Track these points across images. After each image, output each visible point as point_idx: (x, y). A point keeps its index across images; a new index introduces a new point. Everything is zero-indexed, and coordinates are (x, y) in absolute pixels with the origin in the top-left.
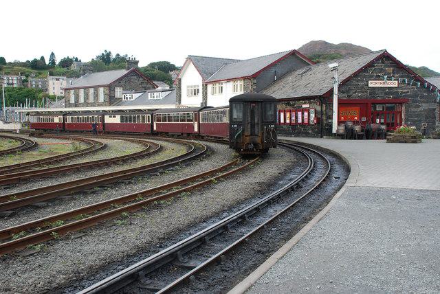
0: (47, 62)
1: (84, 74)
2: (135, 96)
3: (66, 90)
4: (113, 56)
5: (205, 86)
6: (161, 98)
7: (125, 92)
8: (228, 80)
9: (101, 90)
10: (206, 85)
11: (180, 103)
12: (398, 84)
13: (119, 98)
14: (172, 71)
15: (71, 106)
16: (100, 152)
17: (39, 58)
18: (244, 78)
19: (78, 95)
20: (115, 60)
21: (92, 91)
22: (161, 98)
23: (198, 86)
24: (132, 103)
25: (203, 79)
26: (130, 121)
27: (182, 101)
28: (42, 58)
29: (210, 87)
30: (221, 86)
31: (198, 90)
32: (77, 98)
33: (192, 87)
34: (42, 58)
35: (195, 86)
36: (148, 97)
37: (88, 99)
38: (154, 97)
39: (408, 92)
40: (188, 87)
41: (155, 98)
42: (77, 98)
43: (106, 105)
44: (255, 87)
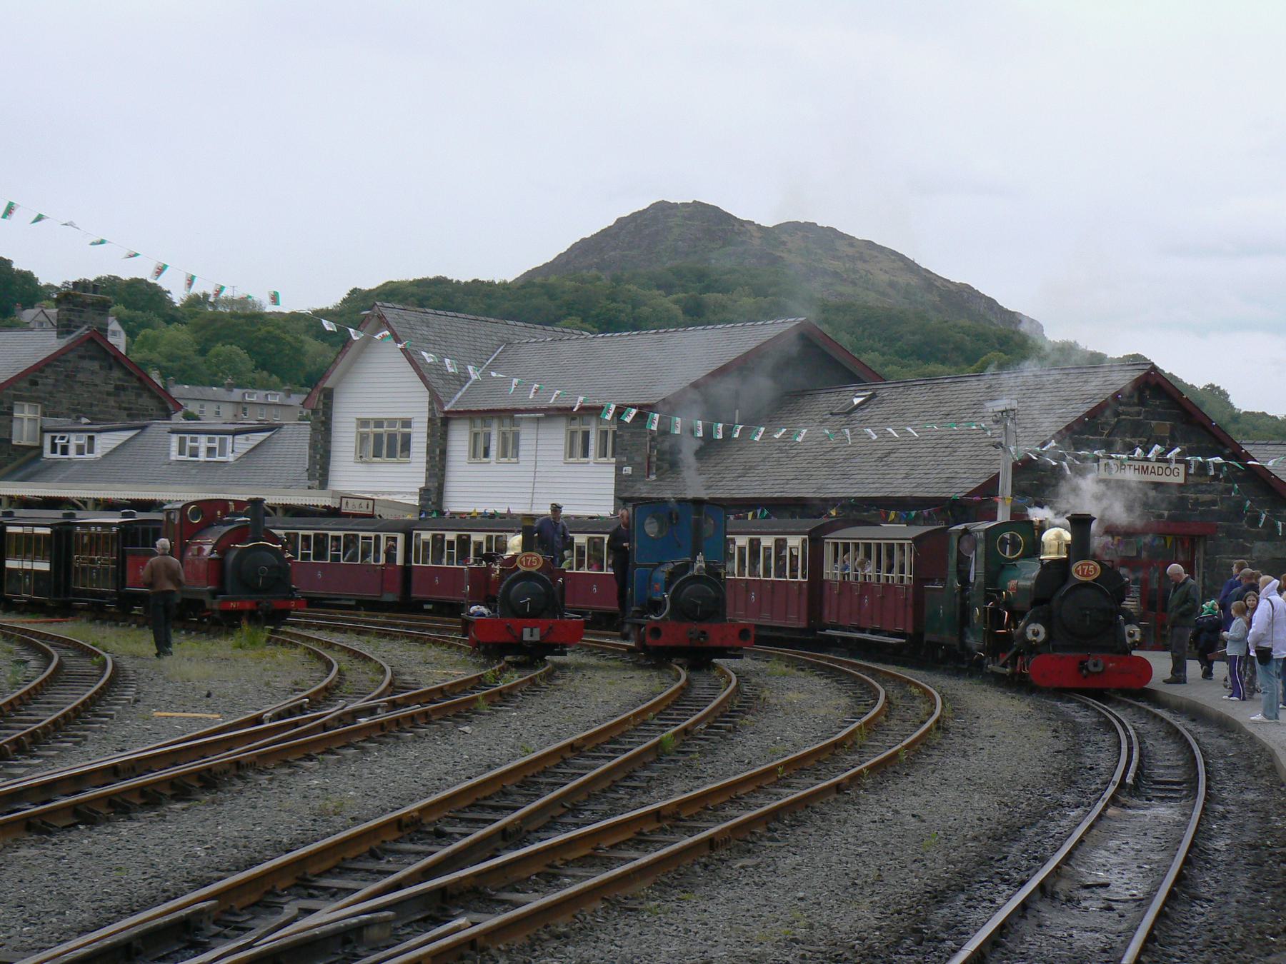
2: (106, 442)
5: (440, 425)
7: (50, 422)
11: (323, 484)
12: (1187, 474)
13: (28, 448)
14: (30, 304)
22: (230, 458)
23: (407, 423)
24: (90, 472)
25: (435, 399)
29: (460, 439)
33: (379, 423)
35: (392, 422)
38: (194, 453)
39: (1214, 503)
40: (364, 423)
41: (202, 457)
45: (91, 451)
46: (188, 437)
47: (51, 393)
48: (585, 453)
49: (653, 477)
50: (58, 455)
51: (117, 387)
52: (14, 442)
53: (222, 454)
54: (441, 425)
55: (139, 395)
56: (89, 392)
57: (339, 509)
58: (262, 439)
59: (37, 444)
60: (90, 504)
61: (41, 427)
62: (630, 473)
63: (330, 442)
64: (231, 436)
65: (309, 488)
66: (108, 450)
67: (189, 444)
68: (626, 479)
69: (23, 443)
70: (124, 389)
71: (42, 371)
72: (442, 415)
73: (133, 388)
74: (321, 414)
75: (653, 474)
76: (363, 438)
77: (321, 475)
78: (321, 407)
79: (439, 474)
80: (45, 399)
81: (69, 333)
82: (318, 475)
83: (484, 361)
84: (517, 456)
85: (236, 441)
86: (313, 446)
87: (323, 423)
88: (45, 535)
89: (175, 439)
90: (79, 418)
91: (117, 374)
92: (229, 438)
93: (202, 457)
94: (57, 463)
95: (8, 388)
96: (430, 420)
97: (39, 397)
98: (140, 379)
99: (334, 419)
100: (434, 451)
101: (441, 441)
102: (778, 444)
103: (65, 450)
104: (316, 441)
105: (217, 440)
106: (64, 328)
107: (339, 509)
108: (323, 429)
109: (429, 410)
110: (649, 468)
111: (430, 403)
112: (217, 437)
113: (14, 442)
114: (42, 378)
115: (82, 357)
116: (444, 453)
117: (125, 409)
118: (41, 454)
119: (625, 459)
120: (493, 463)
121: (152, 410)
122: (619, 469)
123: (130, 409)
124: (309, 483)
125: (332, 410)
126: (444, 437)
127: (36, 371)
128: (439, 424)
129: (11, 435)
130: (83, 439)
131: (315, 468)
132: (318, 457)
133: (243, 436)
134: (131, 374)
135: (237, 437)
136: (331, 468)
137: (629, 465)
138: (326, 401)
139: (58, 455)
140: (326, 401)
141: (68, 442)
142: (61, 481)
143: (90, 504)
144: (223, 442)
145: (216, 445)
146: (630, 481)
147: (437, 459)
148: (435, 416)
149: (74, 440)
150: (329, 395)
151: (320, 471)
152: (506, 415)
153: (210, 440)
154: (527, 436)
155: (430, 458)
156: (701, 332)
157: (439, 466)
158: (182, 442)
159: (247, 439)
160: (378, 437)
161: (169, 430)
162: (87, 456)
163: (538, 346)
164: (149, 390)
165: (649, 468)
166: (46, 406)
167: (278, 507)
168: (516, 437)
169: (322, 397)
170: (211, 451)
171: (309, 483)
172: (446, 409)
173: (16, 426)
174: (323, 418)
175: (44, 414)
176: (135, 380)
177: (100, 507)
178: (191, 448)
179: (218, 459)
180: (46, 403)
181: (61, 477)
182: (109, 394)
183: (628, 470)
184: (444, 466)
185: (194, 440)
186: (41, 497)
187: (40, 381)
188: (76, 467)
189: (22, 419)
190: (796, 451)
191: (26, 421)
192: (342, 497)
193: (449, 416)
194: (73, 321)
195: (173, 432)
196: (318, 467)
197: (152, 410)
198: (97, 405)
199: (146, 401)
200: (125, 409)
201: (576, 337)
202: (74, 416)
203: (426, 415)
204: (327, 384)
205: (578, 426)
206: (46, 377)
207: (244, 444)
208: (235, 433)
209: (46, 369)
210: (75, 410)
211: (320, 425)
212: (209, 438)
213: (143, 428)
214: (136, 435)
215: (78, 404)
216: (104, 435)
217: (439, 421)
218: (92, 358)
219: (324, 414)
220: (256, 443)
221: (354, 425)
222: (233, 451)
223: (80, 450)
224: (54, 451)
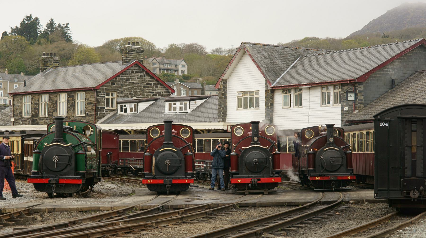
1: (45, 68)
2: (142, 106)
3: (15, 95)
4: (42, 27)
6: (189, 111)
8: (314, 86)
9: (81, 99)
10: (273, 91)
11: (224, 120)
15: (25, 122)
16: (52, 201)
18: (343, 84)
19: (37, 104)
20: (45, 35)
21: (45, 98)
23: (257, 92)
26: (126, 149)
27: (228, 117)
29: (279, 97)
30: (298, 93)
31: (257, 99)
32: (35, 109)
36: (164, 109)
37: (55, 110)
38: (175, 109)
41: (178, 111)
42: (35, 109)
44: (362, 97)
45: (135, 110)
46: (172, 103)
47: (120, 87)
48: (329, 103)
49: (357, 111)
50: (123, 113)
51: (147, 84)
53: (186, 109)
54: (271, 93)
55: (157, 87)
56: (136, 86)
57: (227, 130)
58: (202, 102)
59: (115, 109)
60: (133, 132)
61: (117, 102)
62: (347, 110)
63: (227, 102)
65: (219, 122)
66: (142, 110)
67: (173, 106)
68: (345, 112)
70: (150, 84)
71: (116, 79)
72: (271, 89)
73: (154, 84)
74: (222, 91)
75: (357, 110)
76: (240, 100)
77: (223, 116)
78: (222, 88)
79: (271, 114)
80: (118, 90)
82: (222, 116)
83: (290, 65)
84: (301, 104)
86: (220, 104)
87: (223, 94)
89: (167, 104)
90: (132, 97)
91: (147, 78)
92: (188, 102)
93: (178, 111)
94: (122, 115)
95: (102, 86)
96: (266, 91)
97: (115, 89)
98: (157, 80)
99: (228, 93)
100: (268, 104)
101: (271, 100)
102: (410, 94)
103: (126, 111)
104: (220, 102)
105: (183, 104)
106: (126, 61)
107: (227, 130)
108: (223, 97)
109: (266, 87)
110: (355, 107)
111: (266, 84)
112: (183, 102)
114: (116, 81)
115: (133, 72)
116: (272, 104)
117: (151, 93)
118: (117, 113)
119: (345, 104)
120: (292, 108)
121: (162, 93)
122: (343, 108)
123: (153, 93)
124: (219, 120)
125: (227, 89)
126: (272, 98)
127: (114, 79)
128: (270, 93)
130: (132, 106)
131: (221, 113)
132: (222, 109)
133: (194, 102)
134: (153, 78)
135: (191, 102)
136: (227, 113)
137: (347, 106)
138: (224, 85)
139: (123, 113)
140: (224, 85)
142: (123, 123)
143: (133, 132)
144: (186, 105)
145: (183, 105)
146: (347, 113)
147: (270, 107)
148: (268, 89)
149: (129, 106)
150: (225, 82)
151: (223, 115)
152: (297, 88)
153: (181, 104)
154: (306, 95)
155: (267, 107)
156: (380, 47)
157: (271, 110)
158: (170, 105)
159: (196, 103)
160: (246, 99)
161: (165, 100)
162: (134, 112)
163: (313, 57)
164: (161, 85)
165: (355, 107)
166: (118, 93)
167: (205, 130)
168: (301, 95)
169: (222, 83)
171: (219, 120)
172: (272, 86)
174: (223, 92)
175: (118, 96)
176: (155, 81)
177: (137, 133)
178: (173, 107)
179: (184, 111)
180: (119, 92)
181: (123, 122)
182: (144, 87)
183: (346, 109)
184: (273, 110)
185: (175, 104)
186: (114, 130)
188: (129, 117)
190: (416, 97)
192: (228, 125)
193: (274, 89)
194: (128, 57)
195: (167, 101)
196: (222, 113)
197: (162, 93)
198: (139, 92)
199: (160, 89)
200: (151, 93)
201: (329, 52)
202: (130, 96)
203: (264, 89)
204: (225, 78)
205: (325, 90)
206: (118, 81)
207: (194, 105)
208: (190, 100)
209: (118, 77)
210: (130, 94)
211: (222, 95)
212: (180, 103)
213: (156, 100)
214: (155, 102)
215: (132, 92)
216: (140, 104)
217: (270, 91)
218: (136, 72)
219: (224, 90)
220: (199, 104)
221: (236, 94)
222: (190, 108)
223: (131, 110)
224: (121, 111)
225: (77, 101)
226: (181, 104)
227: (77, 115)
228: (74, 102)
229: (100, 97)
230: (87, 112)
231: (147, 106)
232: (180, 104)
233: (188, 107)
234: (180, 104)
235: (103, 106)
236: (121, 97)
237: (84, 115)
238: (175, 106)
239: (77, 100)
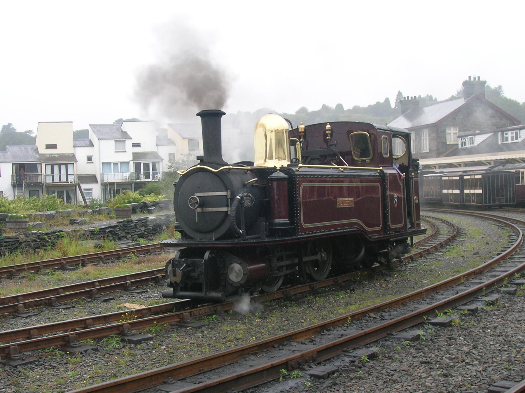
0: (393, 105)
17: (382, 101)
28: (387, 100)
34: (387, 100)
43: (431, 157)
52: (448, 143)
53: (517, 138)
64: (519, 131)
69: (452, 143)
81: (469, 97)
85: (521, 132)
88: (479, 179)
90: (475, 131)
92: (518, 131)
112: (514, 132)
113: (448, 143)
129: (446, 140)
135: (521, 131)
141: (465, 141)
144: (516, 134)
145: (514, 135)
153: (512, 133)
170: (512, 138)
173: (448, 137)
175: (460, 131)
179: (515, 141)
187: (457, 118)
189: (450, 133)
191: (452, 134)
212: (511, 133)
222: (520, 137)
225: (423, 138)
226: (512, 133)
227: (423, 152)
228: (420, 139)
229: (441, 132)
230: (430, 148)
231: (485, 139)
232: (511, 134)
233: (519, 137)
234: (511, 134)
235: (445, 141)
236: (463, 131)
237: (428, 151)
238: (506, 136)
239: (423, 136)
